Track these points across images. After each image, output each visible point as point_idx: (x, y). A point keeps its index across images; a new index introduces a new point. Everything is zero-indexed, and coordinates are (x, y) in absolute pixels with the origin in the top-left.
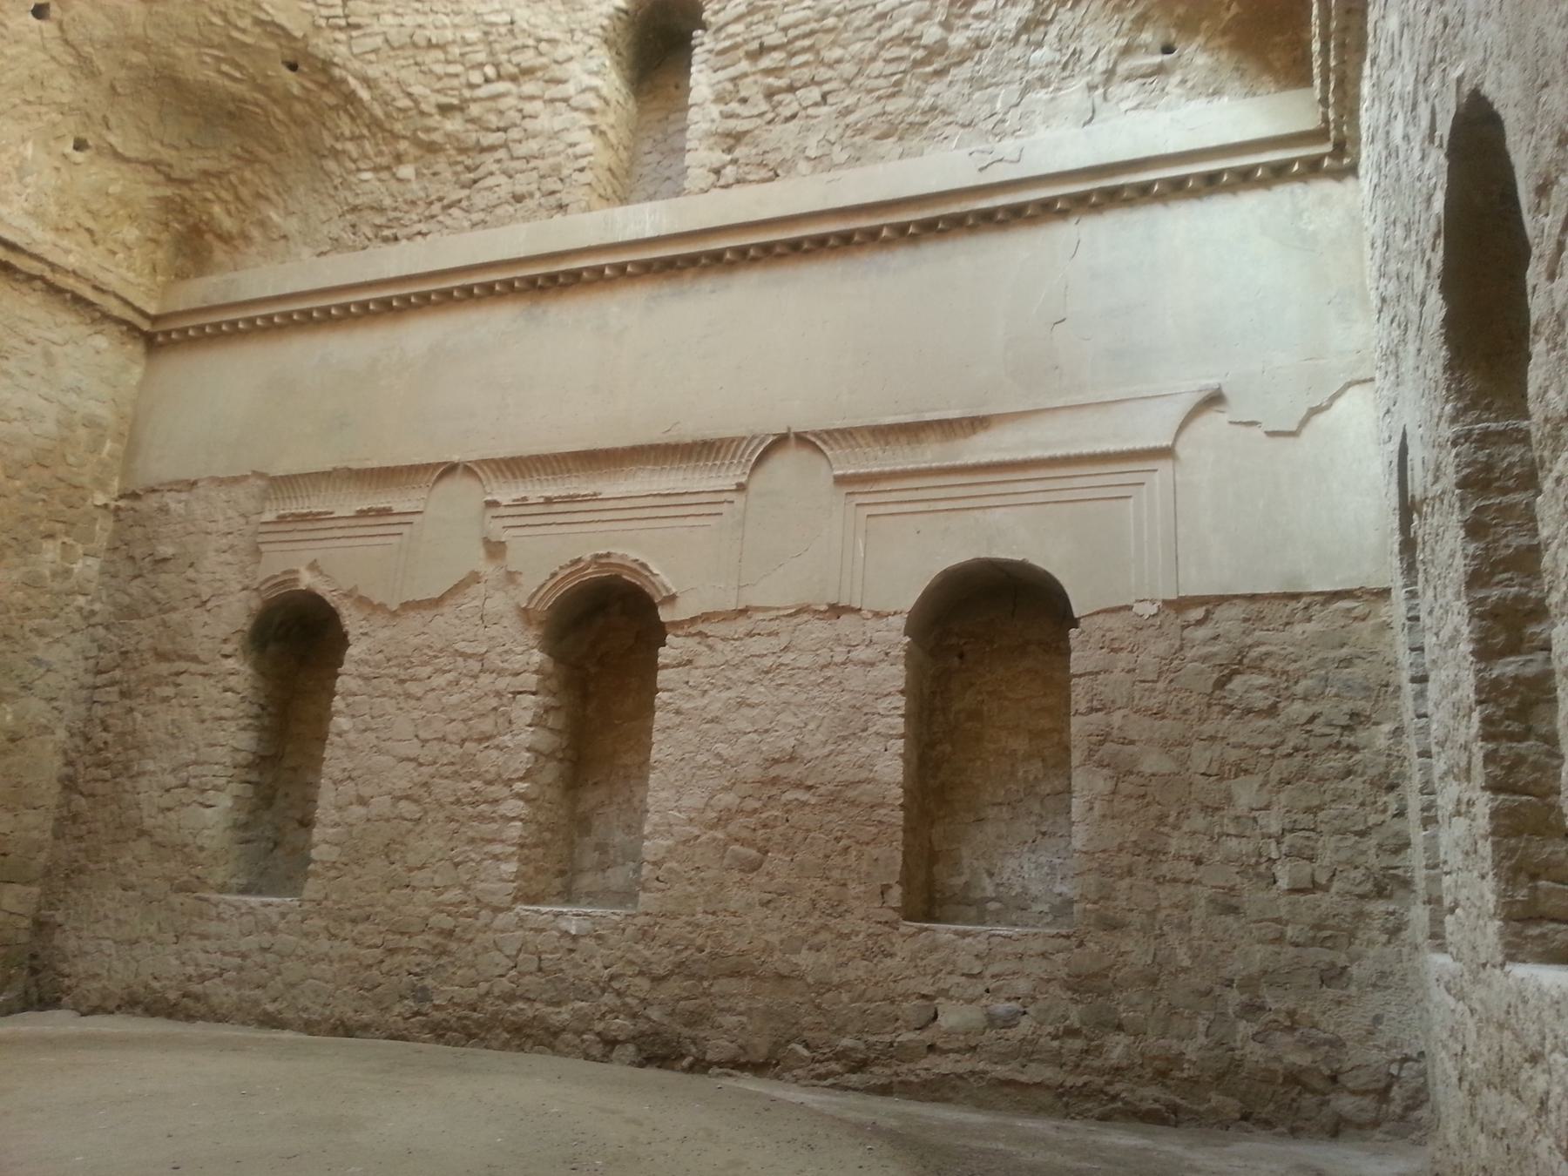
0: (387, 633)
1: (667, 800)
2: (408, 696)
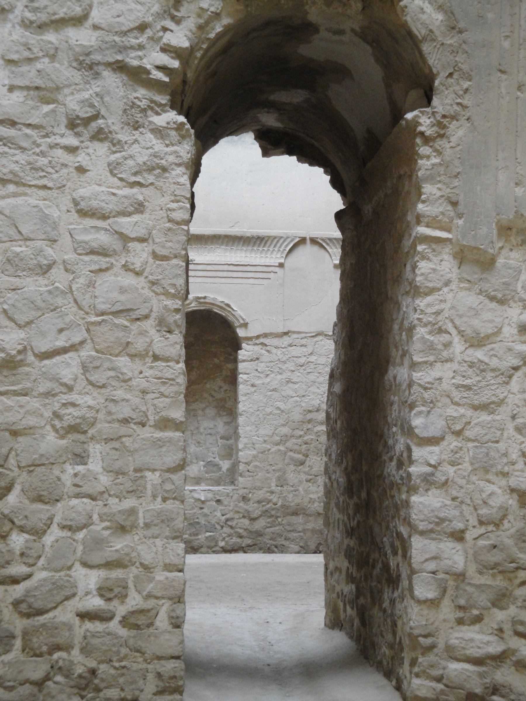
1: (251, 431)
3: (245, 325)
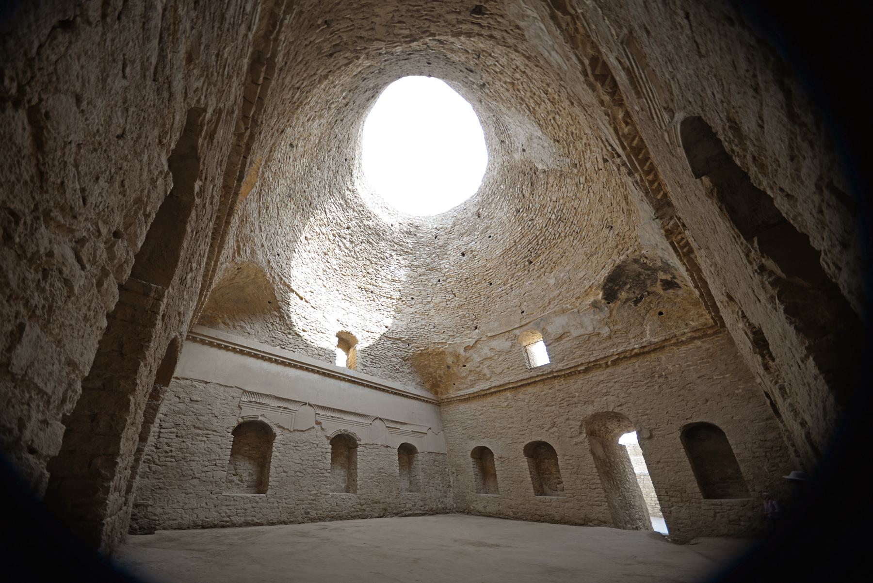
0: (288, 435)
3: (360, 440)
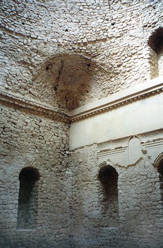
0: (126, 172)
2: (133, 185)
